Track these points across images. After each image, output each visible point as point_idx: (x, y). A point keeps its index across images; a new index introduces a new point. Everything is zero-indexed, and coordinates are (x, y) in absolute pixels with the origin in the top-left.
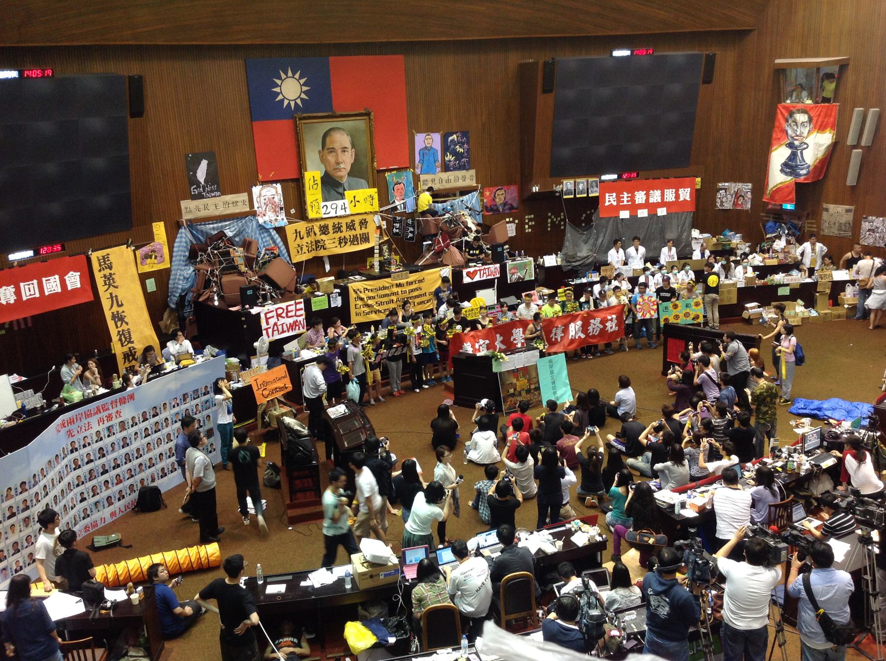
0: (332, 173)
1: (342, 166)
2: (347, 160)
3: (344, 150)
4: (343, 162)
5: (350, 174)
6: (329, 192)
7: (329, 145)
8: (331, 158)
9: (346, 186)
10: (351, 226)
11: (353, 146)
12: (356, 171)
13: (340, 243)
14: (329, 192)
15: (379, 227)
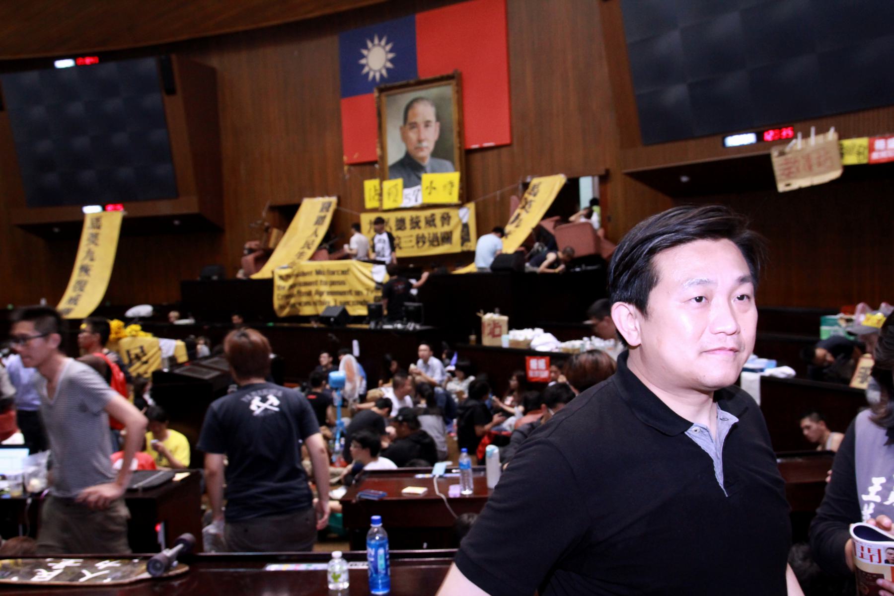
0: (413, 153)
1: (425, 144)
2: (430, 137)
3: (427, 124)
4: (426, 139)
5: (435, 154)
6: (409, 176)
7: (411, 119)
8: (413, 135)
9: (428, 169)
10: (430, 222)
11: (438, 118)
12: (440, 151)
13: (418, 242)
14: (409, 176)
15: (465, 226)
